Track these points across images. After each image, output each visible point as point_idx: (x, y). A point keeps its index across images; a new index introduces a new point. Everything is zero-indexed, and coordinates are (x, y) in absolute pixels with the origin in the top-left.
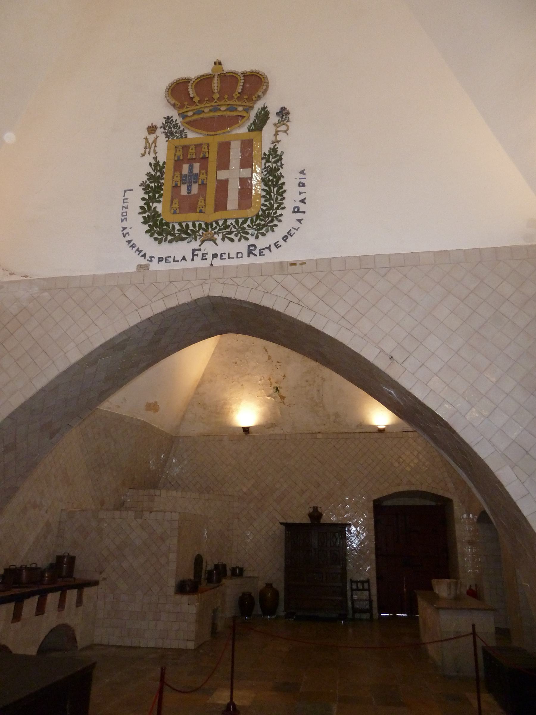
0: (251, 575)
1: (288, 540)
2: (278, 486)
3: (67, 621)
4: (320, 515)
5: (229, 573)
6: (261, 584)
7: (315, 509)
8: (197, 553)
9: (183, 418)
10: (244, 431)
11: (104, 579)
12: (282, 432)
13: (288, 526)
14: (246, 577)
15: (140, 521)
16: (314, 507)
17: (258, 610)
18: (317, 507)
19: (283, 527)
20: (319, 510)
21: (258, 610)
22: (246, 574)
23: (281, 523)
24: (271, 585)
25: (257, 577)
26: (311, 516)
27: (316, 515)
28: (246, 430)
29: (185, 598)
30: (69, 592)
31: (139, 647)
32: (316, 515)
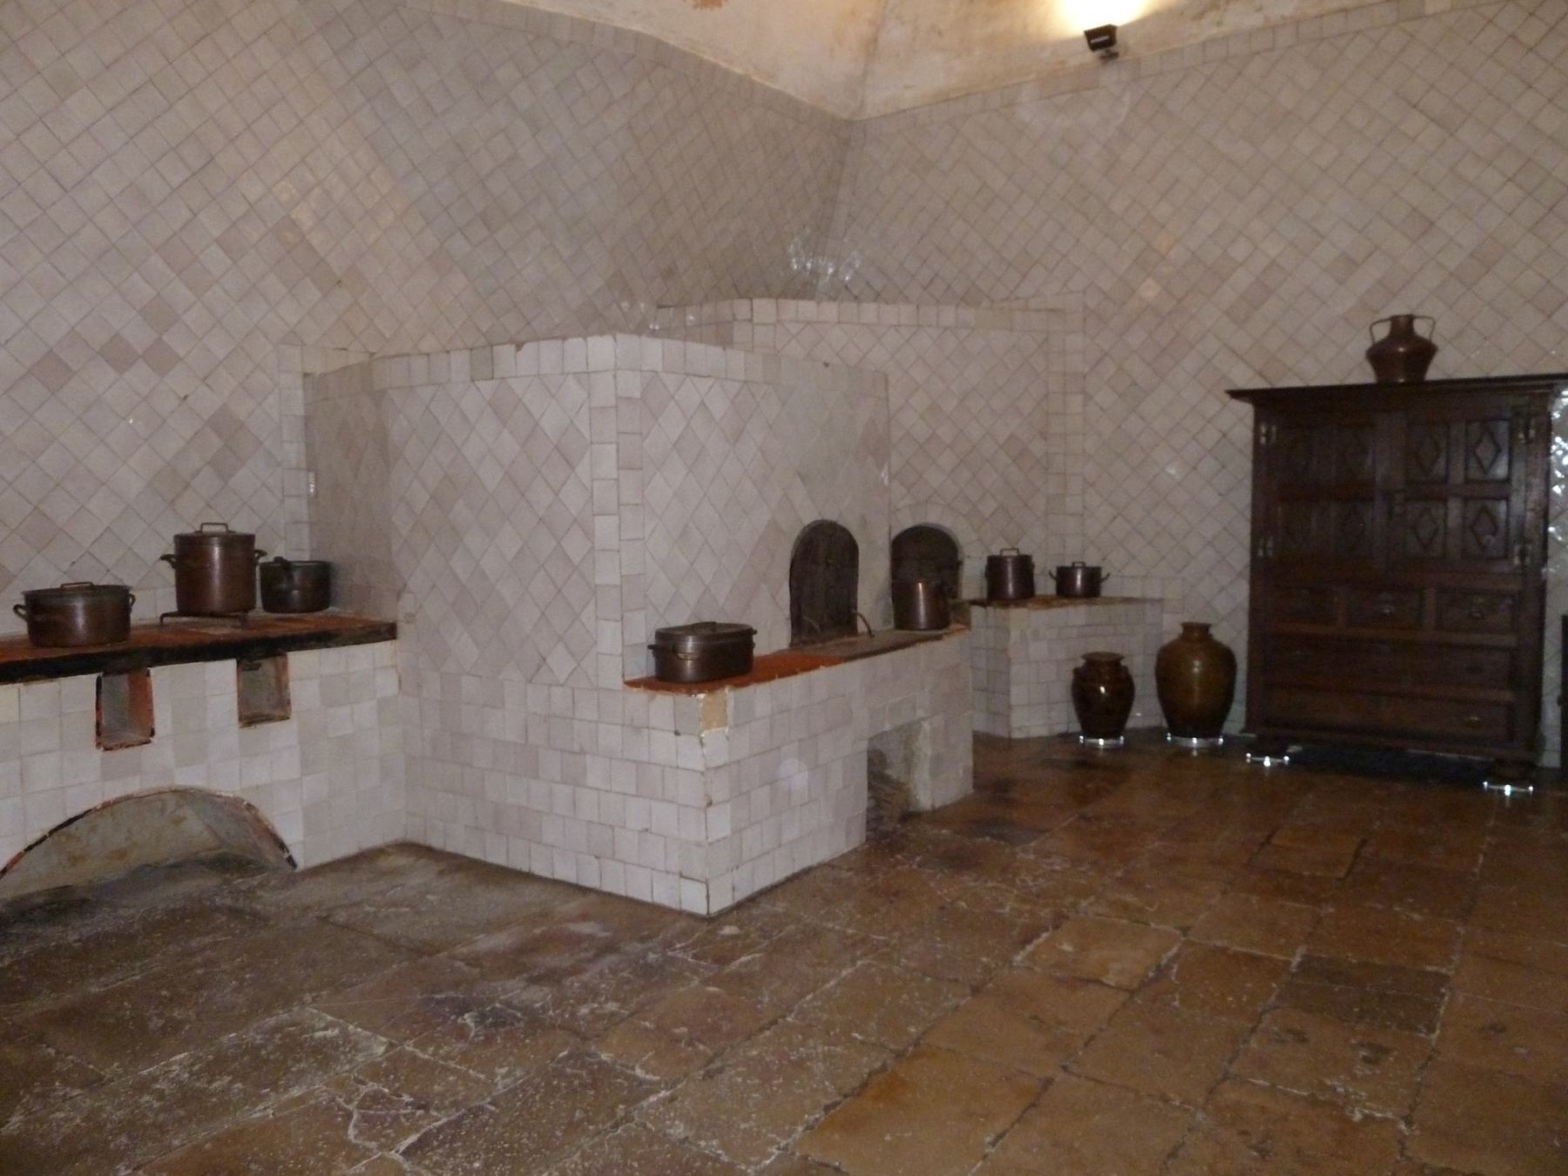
0: (1136, 594)
1: (1263, 457)
2: (1240, 251)
3: (187, 778)
4: (1425, 352)
5: (1045, 585)
6: (1171, 628)
7: (1402, 328)
8: (809, 518)
9: (871, 48)
10: (1094, 47)
11: (410, 618)
12: (1256, 20)
13: (1268, 403)
14: (1111, 601)
15: (487, 387)
16: (1394, 320)
17: (1145, 712)
18: (1410, 319)
19: (1246, 409)
20: (1421, 329)
21: (1145, 712)
22: (1107, 589)
23: (1236, 394)
24: (1204, 629)
25: (1160, 601)
26: (1377, 356)
27: (1403, 351)
28: (1103, 40)
29: (664, 703)
30: (162, 678)
31: (529, 877)
32: (1403, 351)
